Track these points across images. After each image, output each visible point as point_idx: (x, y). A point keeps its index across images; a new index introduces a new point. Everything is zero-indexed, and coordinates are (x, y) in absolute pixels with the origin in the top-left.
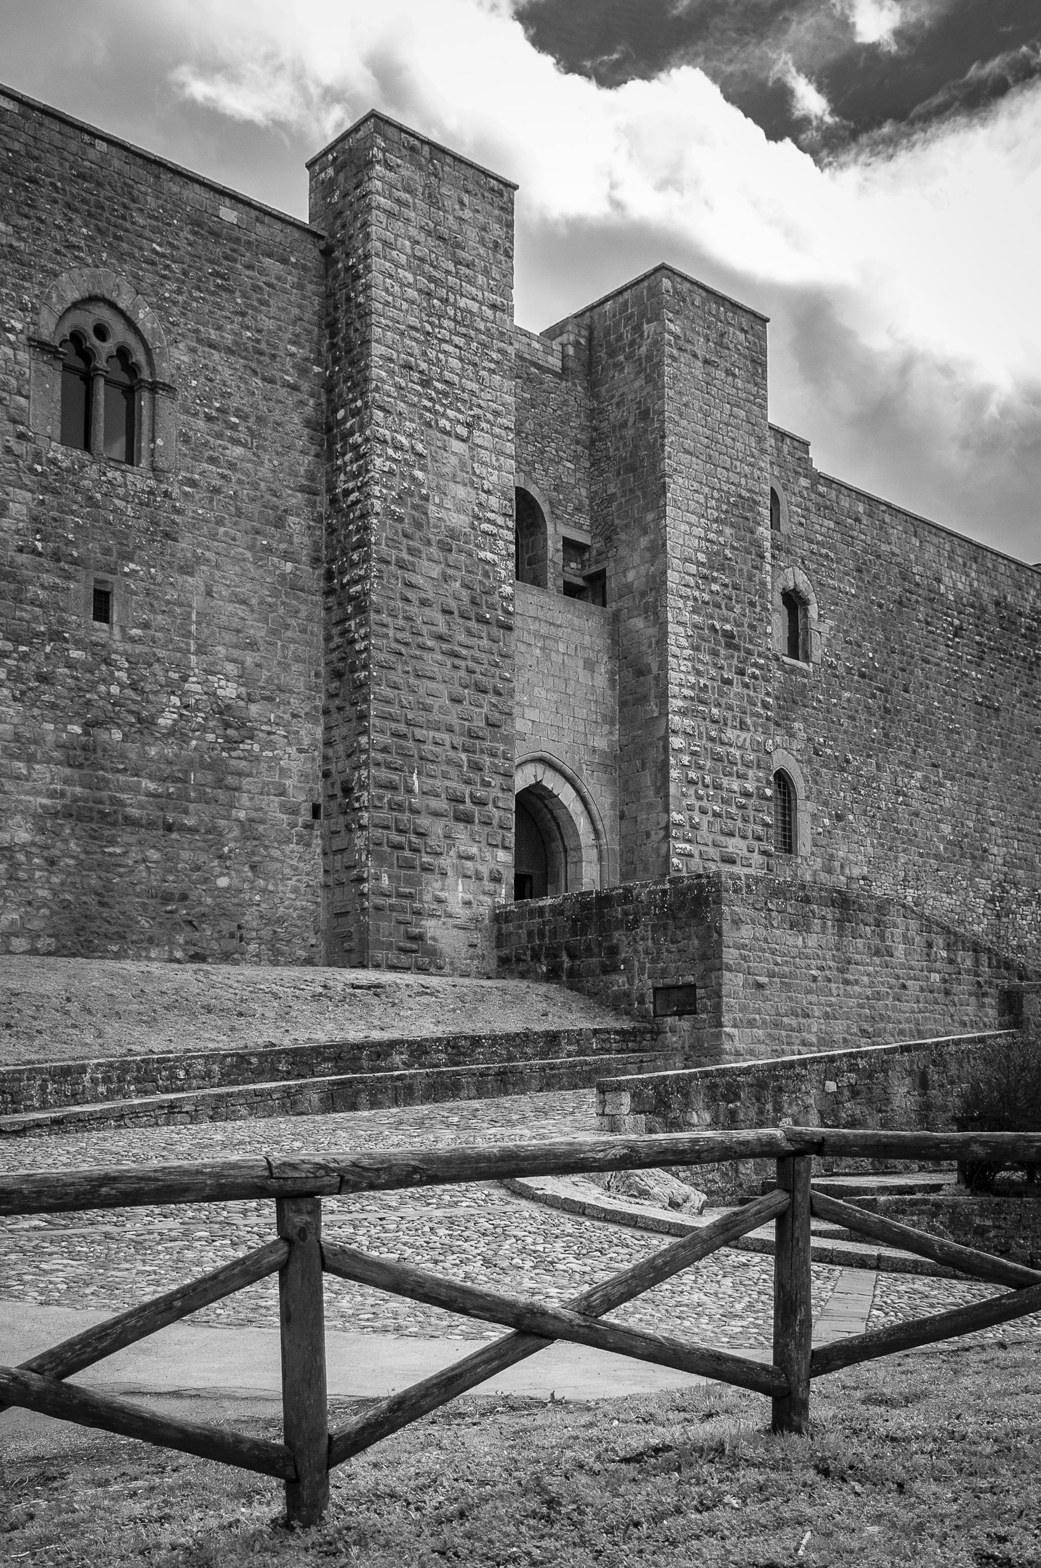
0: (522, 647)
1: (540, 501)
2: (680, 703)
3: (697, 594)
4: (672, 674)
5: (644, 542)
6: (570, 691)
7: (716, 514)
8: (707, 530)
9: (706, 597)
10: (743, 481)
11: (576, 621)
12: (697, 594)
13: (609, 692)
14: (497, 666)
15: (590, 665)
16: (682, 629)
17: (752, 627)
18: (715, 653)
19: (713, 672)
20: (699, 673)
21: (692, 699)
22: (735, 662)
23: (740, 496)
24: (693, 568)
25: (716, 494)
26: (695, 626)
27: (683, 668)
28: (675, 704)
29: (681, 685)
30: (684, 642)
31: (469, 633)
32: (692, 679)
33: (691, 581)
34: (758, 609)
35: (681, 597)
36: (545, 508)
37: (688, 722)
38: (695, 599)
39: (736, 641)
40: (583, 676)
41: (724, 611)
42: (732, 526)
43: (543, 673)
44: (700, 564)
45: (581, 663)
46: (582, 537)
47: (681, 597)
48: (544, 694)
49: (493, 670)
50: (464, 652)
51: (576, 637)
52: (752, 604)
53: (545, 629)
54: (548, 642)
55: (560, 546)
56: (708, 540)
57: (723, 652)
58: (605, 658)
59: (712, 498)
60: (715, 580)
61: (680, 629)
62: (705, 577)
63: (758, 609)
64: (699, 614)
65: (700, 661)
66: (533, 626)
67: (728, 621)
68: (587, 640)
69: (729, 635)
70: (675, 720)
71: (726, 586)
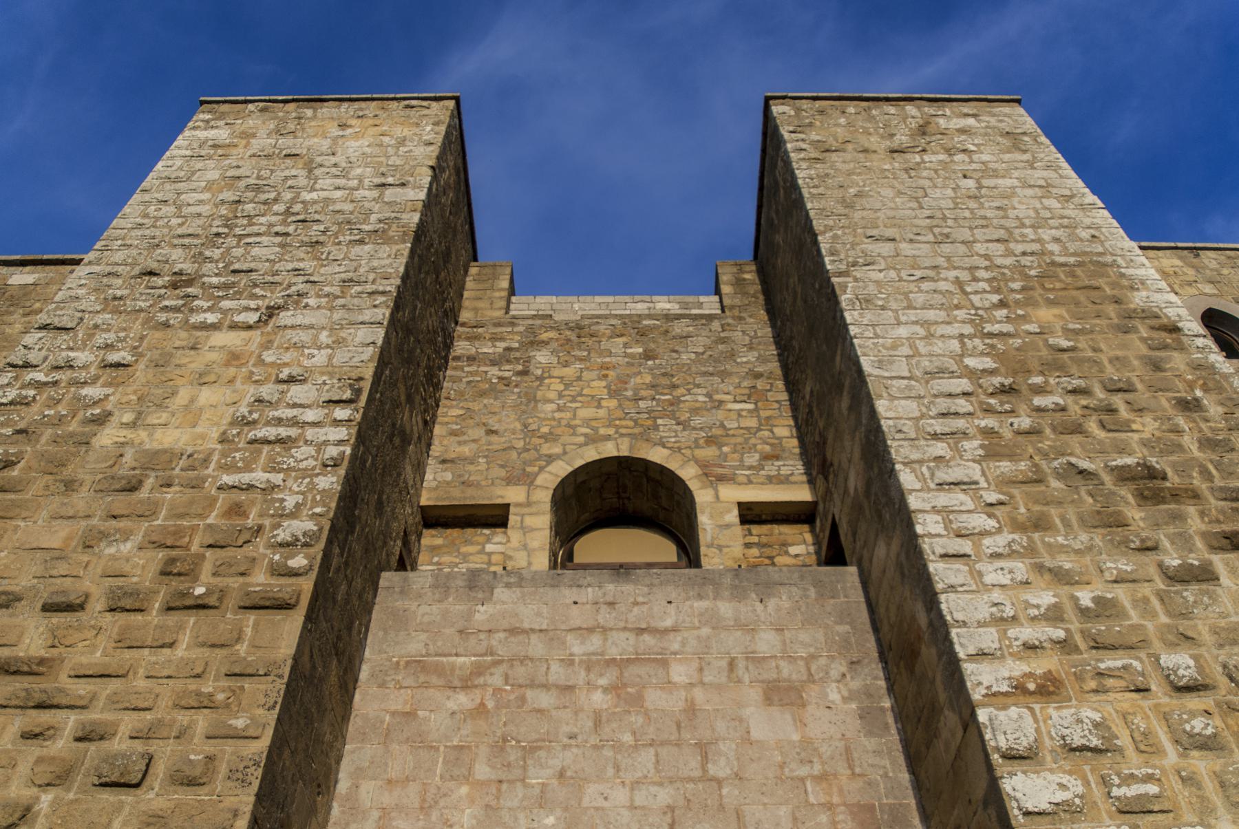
0: (544, 700)
1: (672, 465)
2: (1016, 668)
3: (989, 422)
4: (948, 603)
5: (845, 402)
6: (719, 769)
7: (995, 298)
8: (978, 322)
9: (1025, 422)
10: (1055, 247)
11: (726, 608)
12: (989, 422)
13: (871, 743)
14: (205, 703)
15: (781, 694)
16: (962, 496)
17: (1207, 443)
18: (1113, 522)
19: (1125, 565)
20: (1061, 577)
21: (1065, 645)
22: (1195, 523)
23: (1053, 263)
24: (964, 384)
25: (982, 274)
26: (1005, 483)
27: (989, 579)
28: (981, 678)
29: (1000, 622)
30: (981, 521)
31: (126, 643)
32: (1045, 598)
33: (963, 405)
34: (1214, 410)
35: (935, 436)
36: (688, 473)
37: (1072, 720)
38: (988, 432)
39: (1174, 480)
40: (769, 726)
41: (1101, 434)
42: (1052, 303)
43: (618, 747)
44: (972, 374)
45: (754, 694)
46: (802, 494)
47: (935, 436)
48: (620, 796)
49: (183, 718)
50: (82, 688)
51: (733, 642)
52: (1189, 406)
53: (621, 645)
54: (633, 671)
55: (733, 516)
56: (991, 335)
57: (1135, 514)
58: (839, 667)
59: (975, 279)
60: (1040, 390)
61: (958, 499)
62: (1006, 391)
63: (1214, 410)
64: (1012, 457)
65: (1063, 549)
66: (577, 647)
67: (1122, 450)
68: (766, 642)
69: (1148, 483)
70: (1005, 726)
71: (1074, 391)
